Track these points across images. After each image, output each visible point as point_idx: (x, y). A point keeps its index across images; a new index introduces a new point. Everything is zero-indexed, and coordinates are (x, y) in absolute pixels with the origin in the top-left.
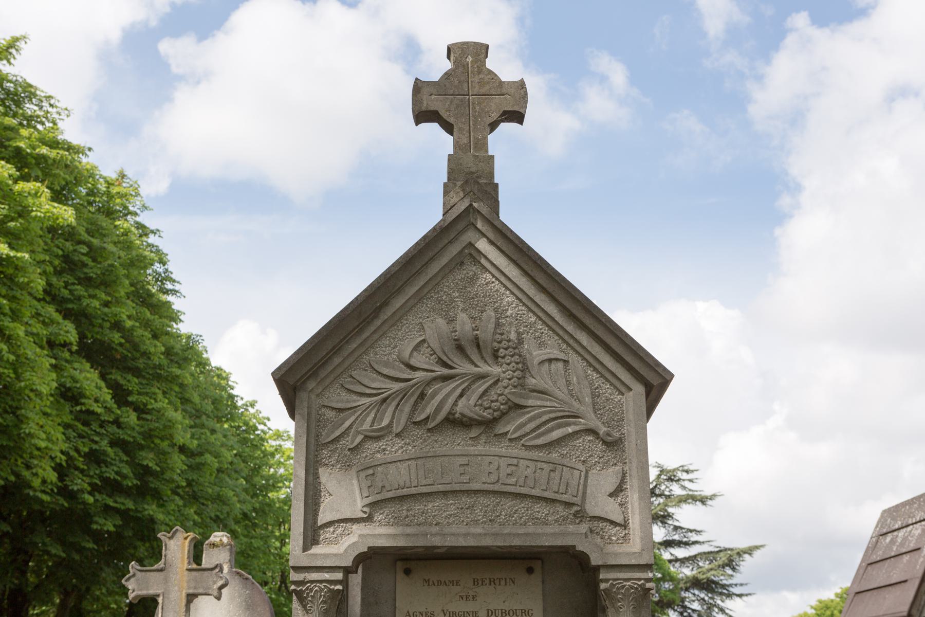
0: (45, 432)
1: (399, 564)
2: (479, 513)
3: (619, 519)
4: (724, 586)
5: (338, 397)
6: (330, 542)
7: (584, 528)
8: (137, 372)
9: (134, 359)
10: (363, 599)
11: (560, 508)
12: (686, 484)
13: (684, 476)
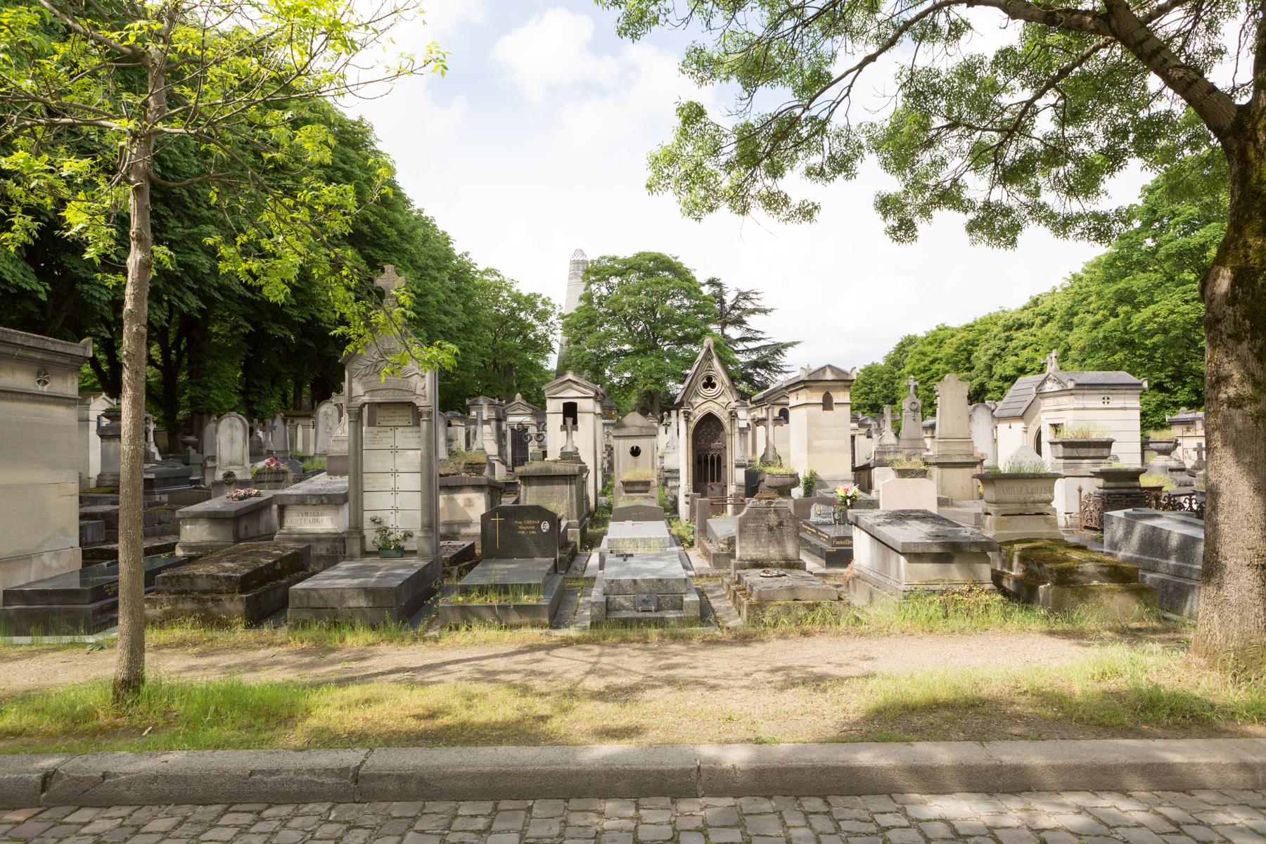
4: (778, 367)
5: (356, 366)
8: (381, 247)
9: (379, 239)
12: (756, 301)
13: (754, 296)
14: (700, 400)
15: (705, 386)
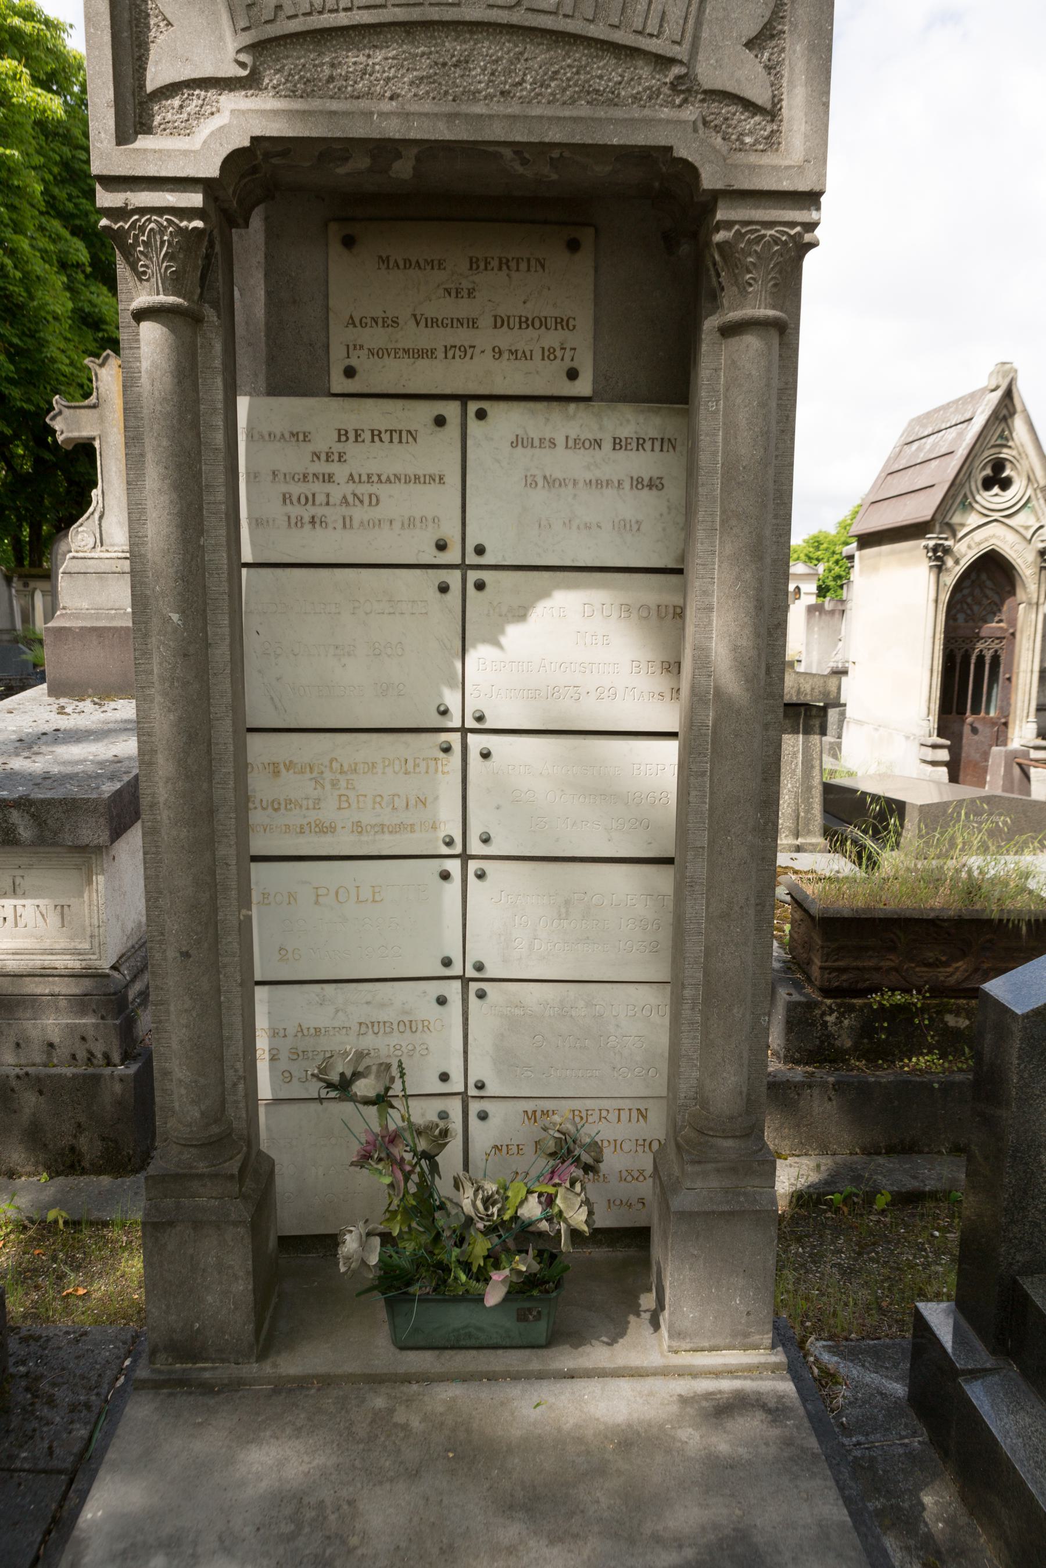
0: (68, 357)
1: (333, 227)
2: (478, 77)
3: (760, 95)
6: (176, 131)
7: (690, 113)
10: (269, 294)
11: (644, 71)
14: (973, 520)
15: (988, 484)
